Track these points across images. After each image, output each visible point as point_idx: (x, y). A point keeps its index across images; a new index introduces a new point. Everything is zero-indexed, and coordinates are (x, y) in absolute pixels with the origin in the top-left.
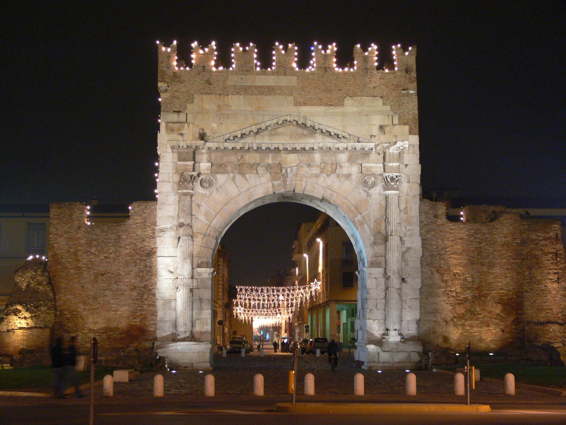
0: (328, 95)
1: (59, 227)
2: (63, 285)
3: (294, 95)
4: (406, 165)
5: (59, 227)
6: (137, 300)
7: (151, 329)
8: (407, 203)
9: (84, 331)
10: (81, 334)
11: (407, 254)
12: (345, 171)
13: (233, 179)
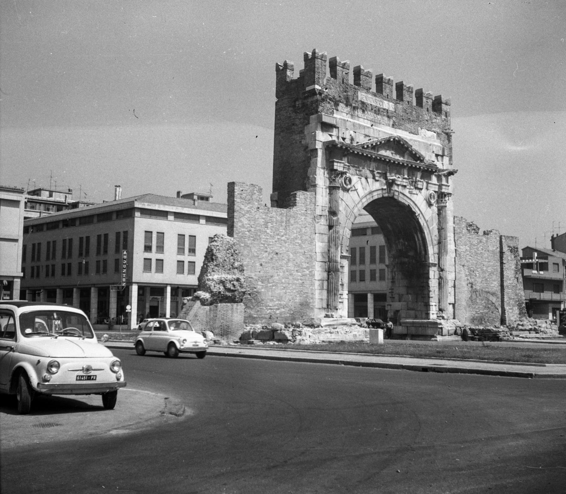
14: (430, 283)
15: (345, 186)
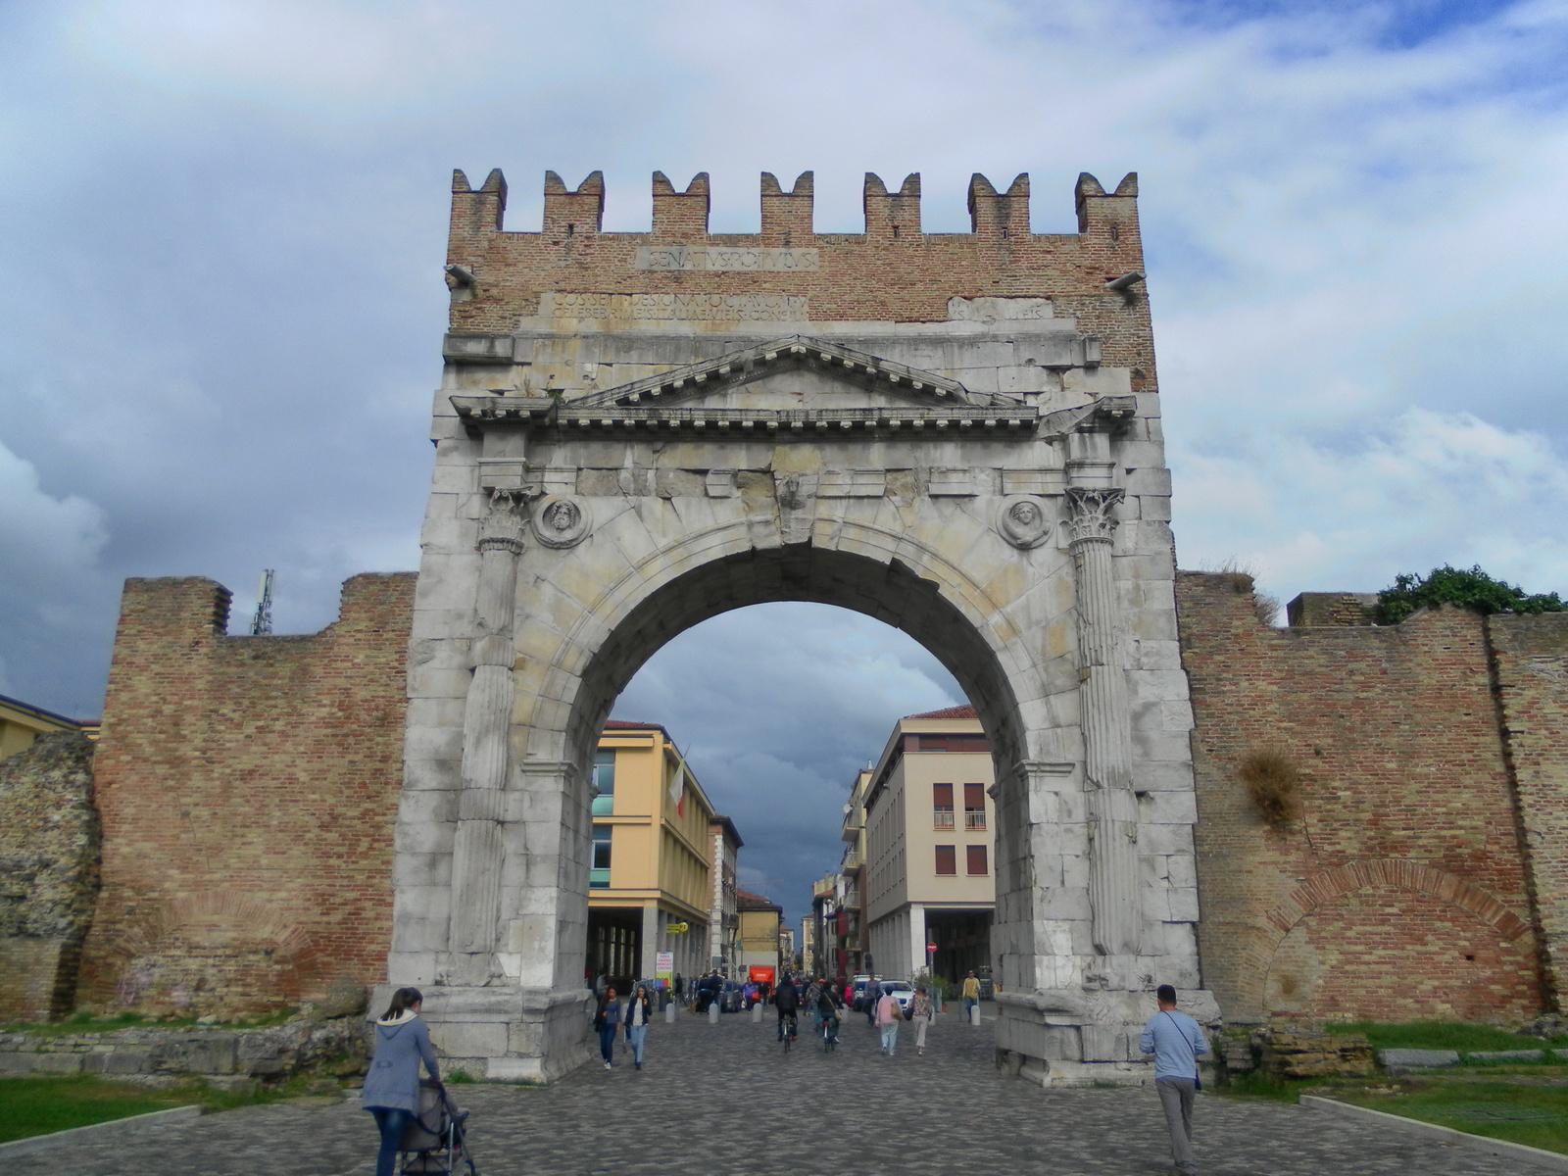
1: (142, 645)
2: (129, 811)
3: (810, 295)
4: (1129, 471)
5: (142, 645)
6: (340, 856)
7: (373, 947)
8: (1137, 576)
9: (173, 952)
10: (161, 960)
11: (1148, 722)
12: (955, 485)
13: (638, 510)
14: (1035, 840)
15: (548, 533)
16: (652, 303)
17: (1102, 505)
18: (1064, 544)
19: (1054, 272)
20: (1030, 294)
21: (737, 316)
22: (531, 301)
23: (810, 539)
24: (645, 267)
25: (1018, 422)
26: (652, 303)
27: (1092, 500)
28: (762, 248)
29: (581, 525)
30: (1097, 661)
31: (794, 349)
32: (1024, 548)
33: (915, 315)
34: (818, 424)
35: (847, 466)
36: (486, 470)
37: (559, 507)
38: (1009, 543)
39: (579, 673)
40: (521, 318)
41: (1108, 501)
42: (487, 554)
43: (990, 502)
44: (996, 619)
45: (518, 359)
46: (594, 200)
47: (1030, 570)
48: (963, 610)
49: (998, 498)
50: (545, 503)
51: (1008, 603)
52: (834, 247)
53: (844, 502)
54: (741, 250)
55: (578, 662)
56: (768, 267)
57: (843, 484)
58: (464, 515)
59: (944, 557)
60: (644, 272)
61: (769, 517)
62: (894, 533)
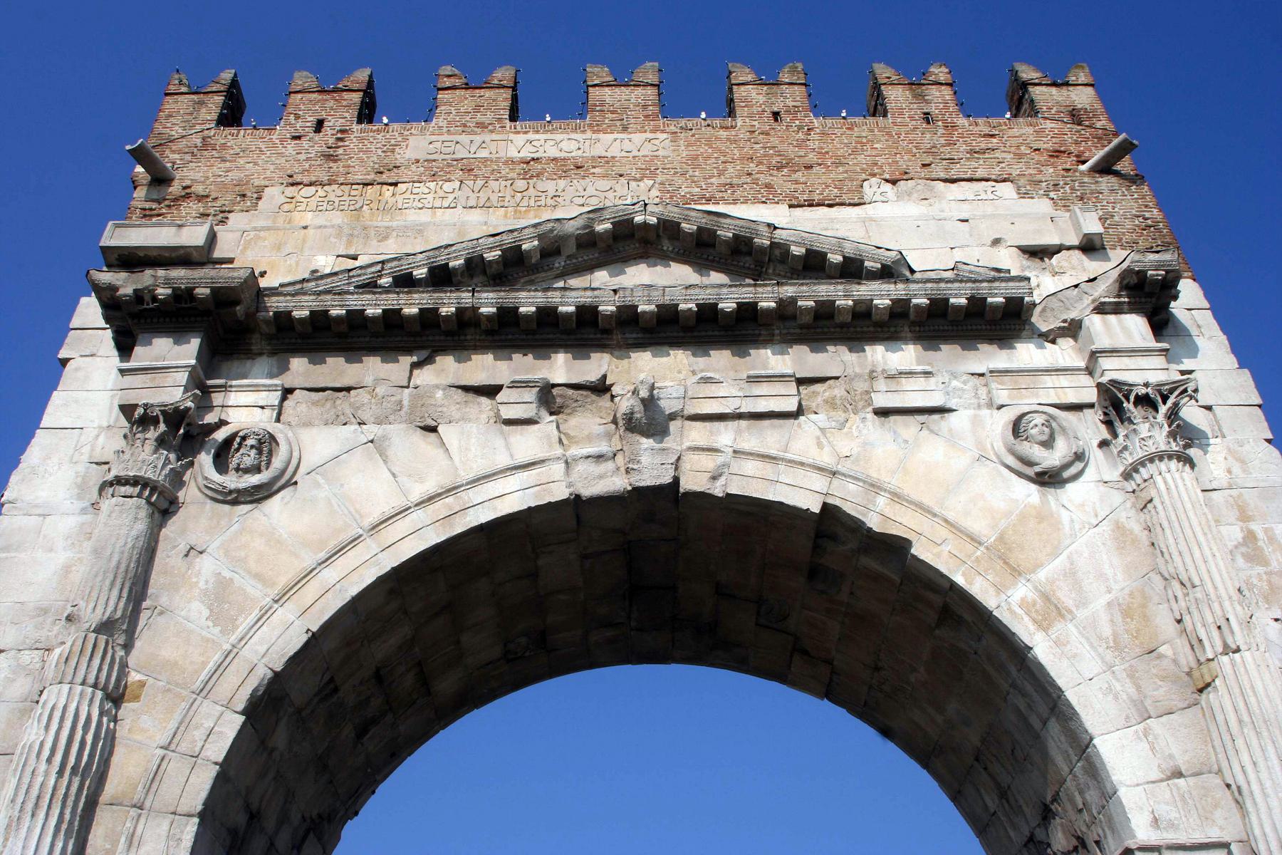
0: (798, 175)
3: (659, 179)
8: (1244, 517)
16: (427, 191)
17: (1163, 409)
18: (1114, 474)
19: (1004, 155)
20: (978, 175)
21: (550, 202)
22: (249, 196)
23: (676, 481)
24: (422, 156)
25: (1002, 300)
26: (427, 191)
27: (1145, 401)
28: (589, 134)
29: (277, 463)
30: (1226, 646)
31: (639, 219)
32: (1049, 479)
33: (816, 198)
34: (682, 306)
35: (732, 374)
36: (129, 380)
37: (244, 438)
38: (1020, 475)
39: (241, 707)
40: (230, 215)
41: (1170, 403)
42: (107, 504)
43: (976, 422)
44: (1021, 591)
45: (217, 254)
46: (356, 97)
47: (1065, 516)
48: (959, 579)
49: (985, 412)
50: (220, 435)
51: (1038, 566)
52: (691, 133)
53: (732, 425)
54: (559, 137)
55: (241, 684)
56: (598, 150)
57: (728, 396)
58: (85, 458)
59: (915, 496)
60: (418, 161)
61: (603, 448)
62: (822, 464)
